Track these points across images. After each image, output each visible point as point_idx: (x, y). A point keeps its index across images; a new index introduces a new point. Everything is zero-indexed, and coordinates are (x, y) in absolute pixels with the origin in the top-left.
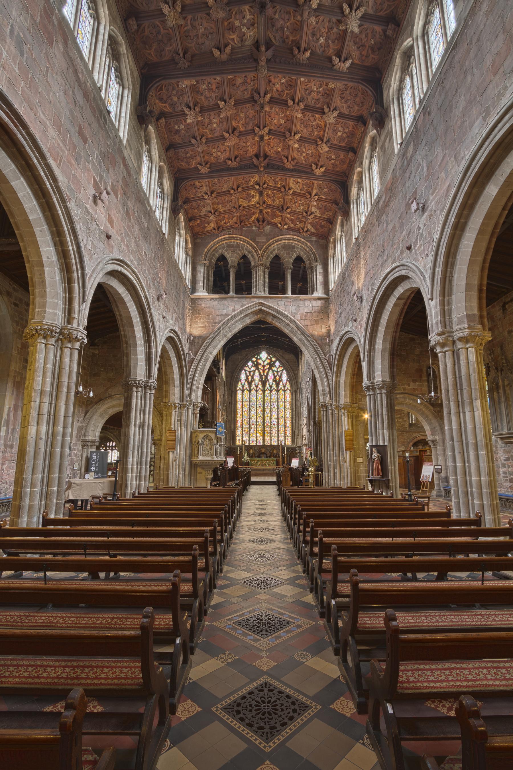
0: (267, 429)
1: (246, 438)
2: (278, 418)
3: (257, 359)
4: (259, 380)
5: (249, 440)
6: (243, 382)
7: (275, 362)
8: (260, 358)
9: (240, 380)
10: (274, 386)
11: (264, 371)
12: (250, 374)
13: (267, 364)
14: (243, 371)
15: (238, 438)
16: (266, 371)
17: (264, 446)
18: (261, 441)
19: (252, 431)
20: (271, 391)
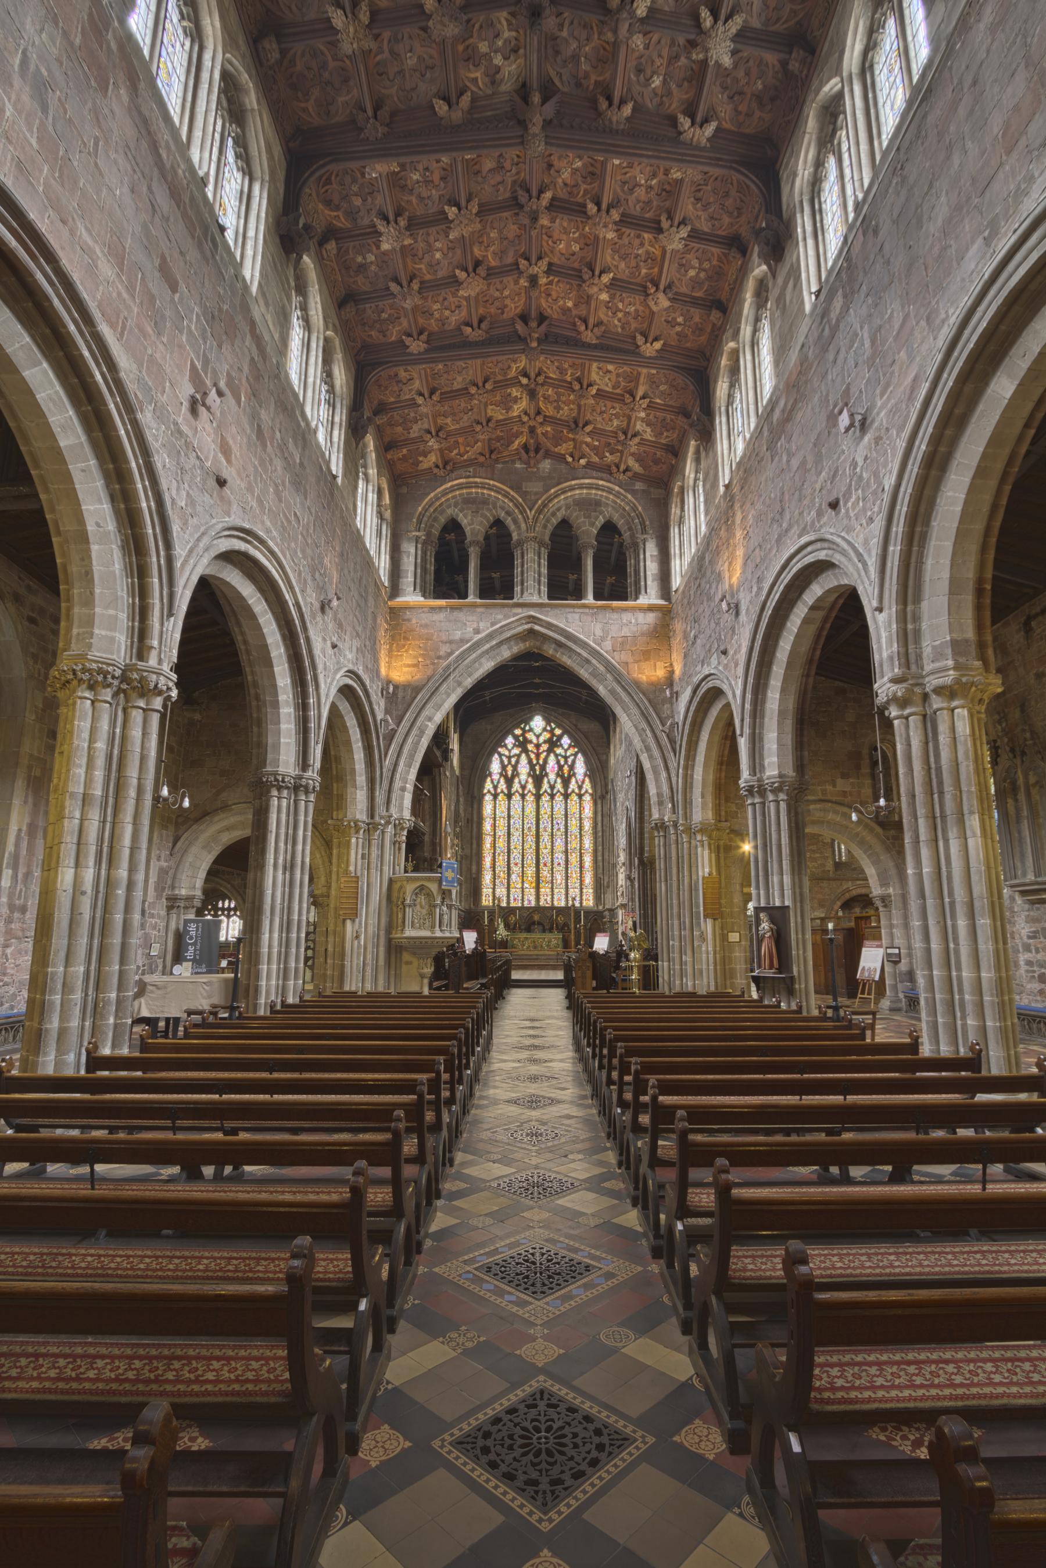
0: (545, 873)
1: (501, 892)
2: (566, 852)
3: (524, 731)
4: (529, 775)
6: (496, 777)
7: (560, 737)
8: (531, 730)
9: (490, 775)
11: (538, 755)
12: (510, 762)
13: (545, 742)
14: (496, 756)
15: (486, 891)
16: (543, 756)
18: (533, 898)
20: (552, 796)
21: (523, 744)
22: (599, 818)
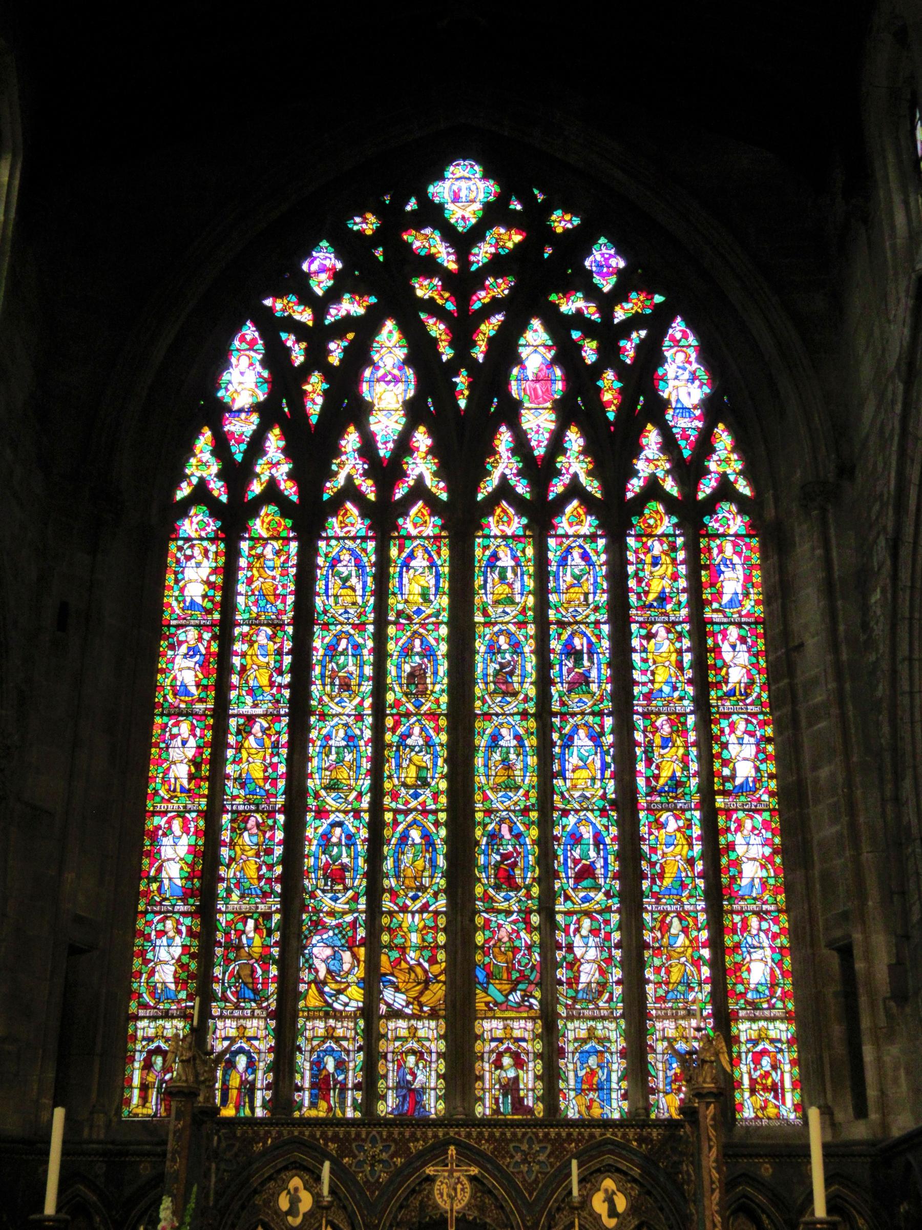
1: (239, 1031)
2: (625, 805)
3: (394, 224)
4: (415, 412)
5: (283, 1064)
7: (579, 242)
8: (433, 215)
9: (215, 413)
10: (575, 463)
11: (463, 328)
12: (316, 359)
13: (497, 266)
14: (250, 331)
16: (489, 328)
17: (460, 1132)
18: (429, 1078)
19: (319, 951)
20: (541, 516)
21: (385, 277)
22: (810, 607)
